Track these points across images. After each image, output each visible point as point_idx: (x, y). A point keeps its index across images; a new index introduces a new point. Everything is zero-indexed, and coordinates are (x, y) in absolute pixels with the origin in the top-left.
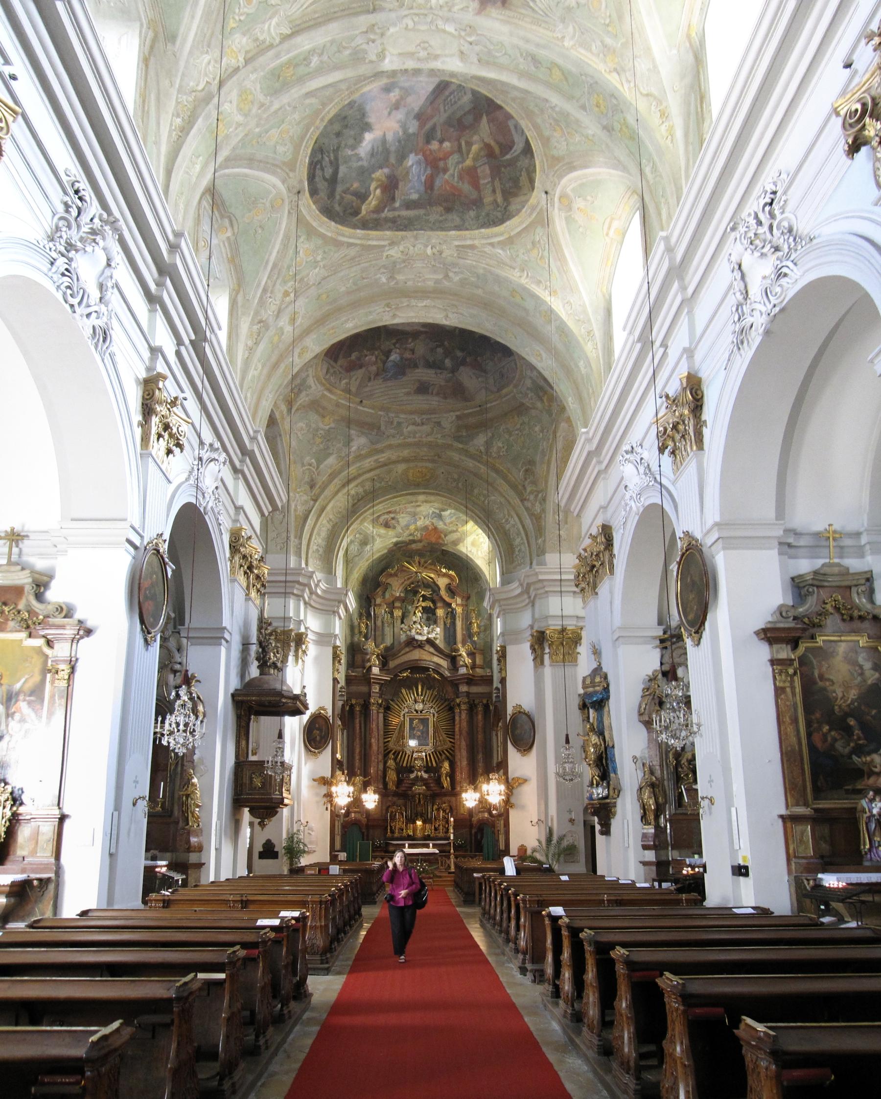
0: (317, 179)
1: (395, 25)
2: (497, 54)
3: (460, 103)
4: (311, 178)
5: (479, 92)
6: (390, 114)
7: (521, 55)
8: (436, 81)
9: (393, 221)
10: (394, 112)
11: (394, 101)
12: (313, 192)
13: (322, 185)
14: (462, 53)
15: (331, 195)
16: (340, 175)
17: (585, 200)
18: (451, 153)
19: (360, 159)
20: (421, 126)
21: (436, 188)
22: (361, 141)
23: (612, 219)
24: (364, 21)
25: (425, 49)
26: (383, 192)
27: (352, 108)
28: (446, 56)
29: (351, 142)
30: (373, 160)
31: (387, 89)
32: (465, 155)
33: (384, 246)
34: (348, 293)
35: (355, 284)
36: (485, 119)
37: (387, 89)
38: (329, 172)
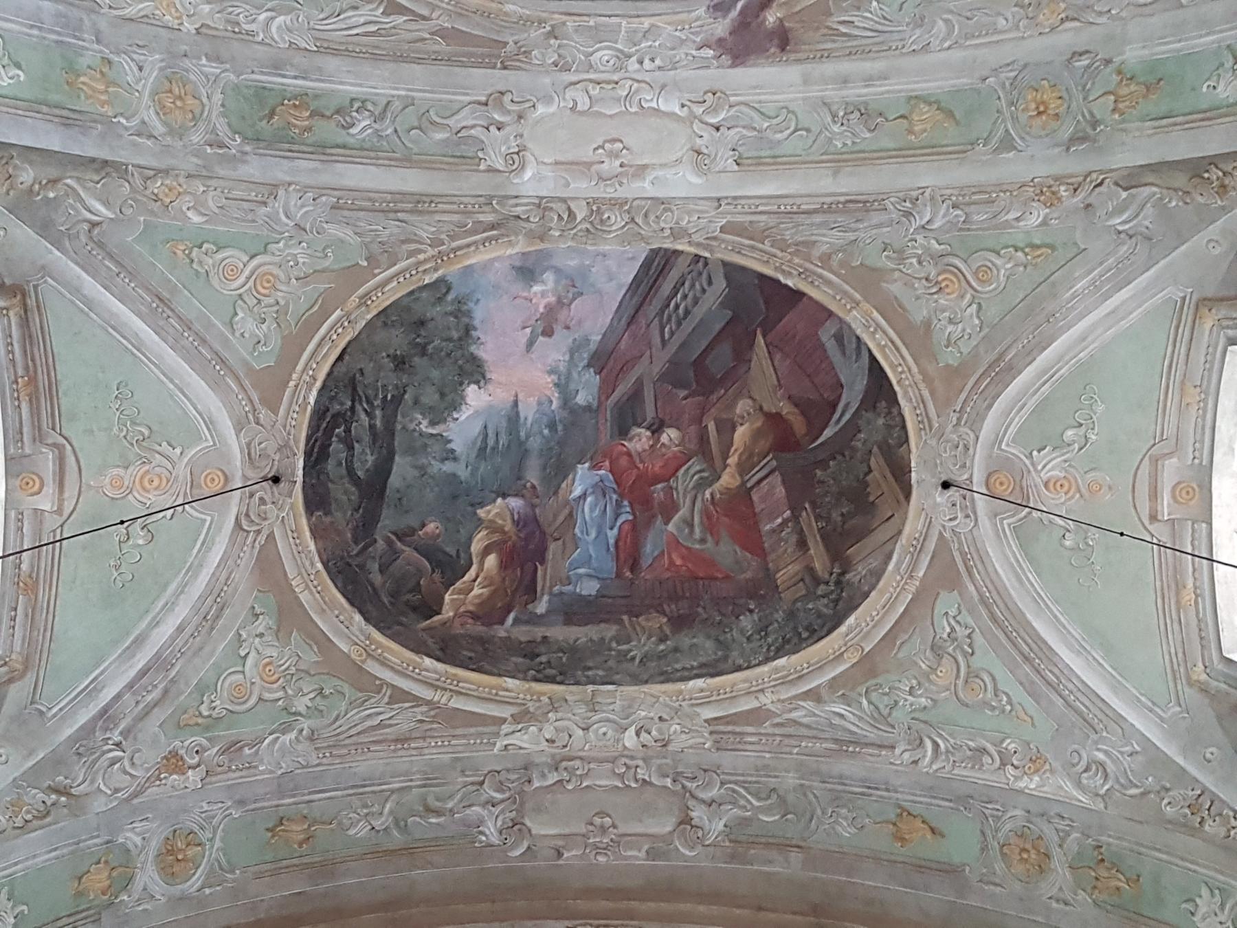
0: (330, 465)
1: (548, 100)
2: (779, 136)
3: (699, 312)
4: (316, 456)
5: (743, 269)
6: (530, 344)
7: (834, 116)
8: (641, 252)
9: (530, 651)
10: (541, 338)
11: (541, 310)
12: (316, 500)
13: (343, 493)
14: (699, 153)
15: (365, 528)
16: (394, 481)
17: (1061, 445)
18: (683, 460)
19: (451, 456)
20: (607, 388)
21: (645, 562)
22: (455, 406)
23: (1155, 461)
24: (484, 80)
25: (614, 155)
26: (503, 565)
27: (440, 300)
28: (663, 166)
29: (430, 397)
30: (483, 468)
31: (527, 272)
32: (718, 463)
33: (504, 720)
34: (380, 854)
35: (400, 823)
36: (760, 340)
37: (527, 272)
38: (366, 459)
